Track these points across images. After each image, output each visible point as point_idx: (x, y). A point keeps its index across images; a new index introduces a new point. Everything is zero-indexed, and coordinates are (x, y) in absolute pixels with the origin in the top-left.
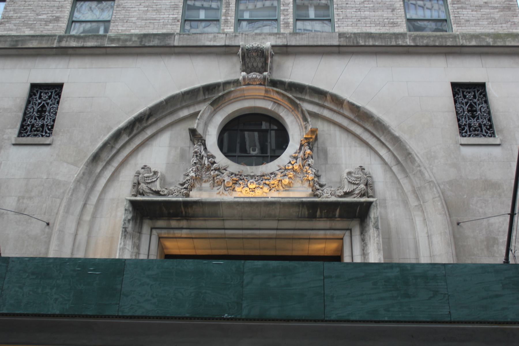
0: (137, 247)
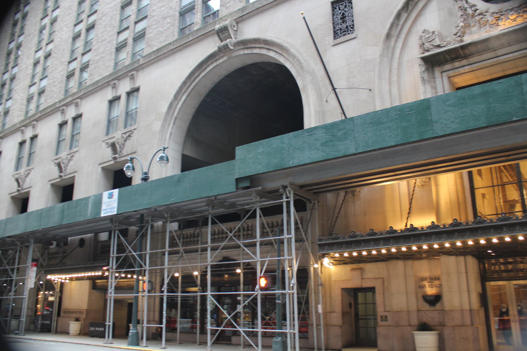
0: (435, 88)
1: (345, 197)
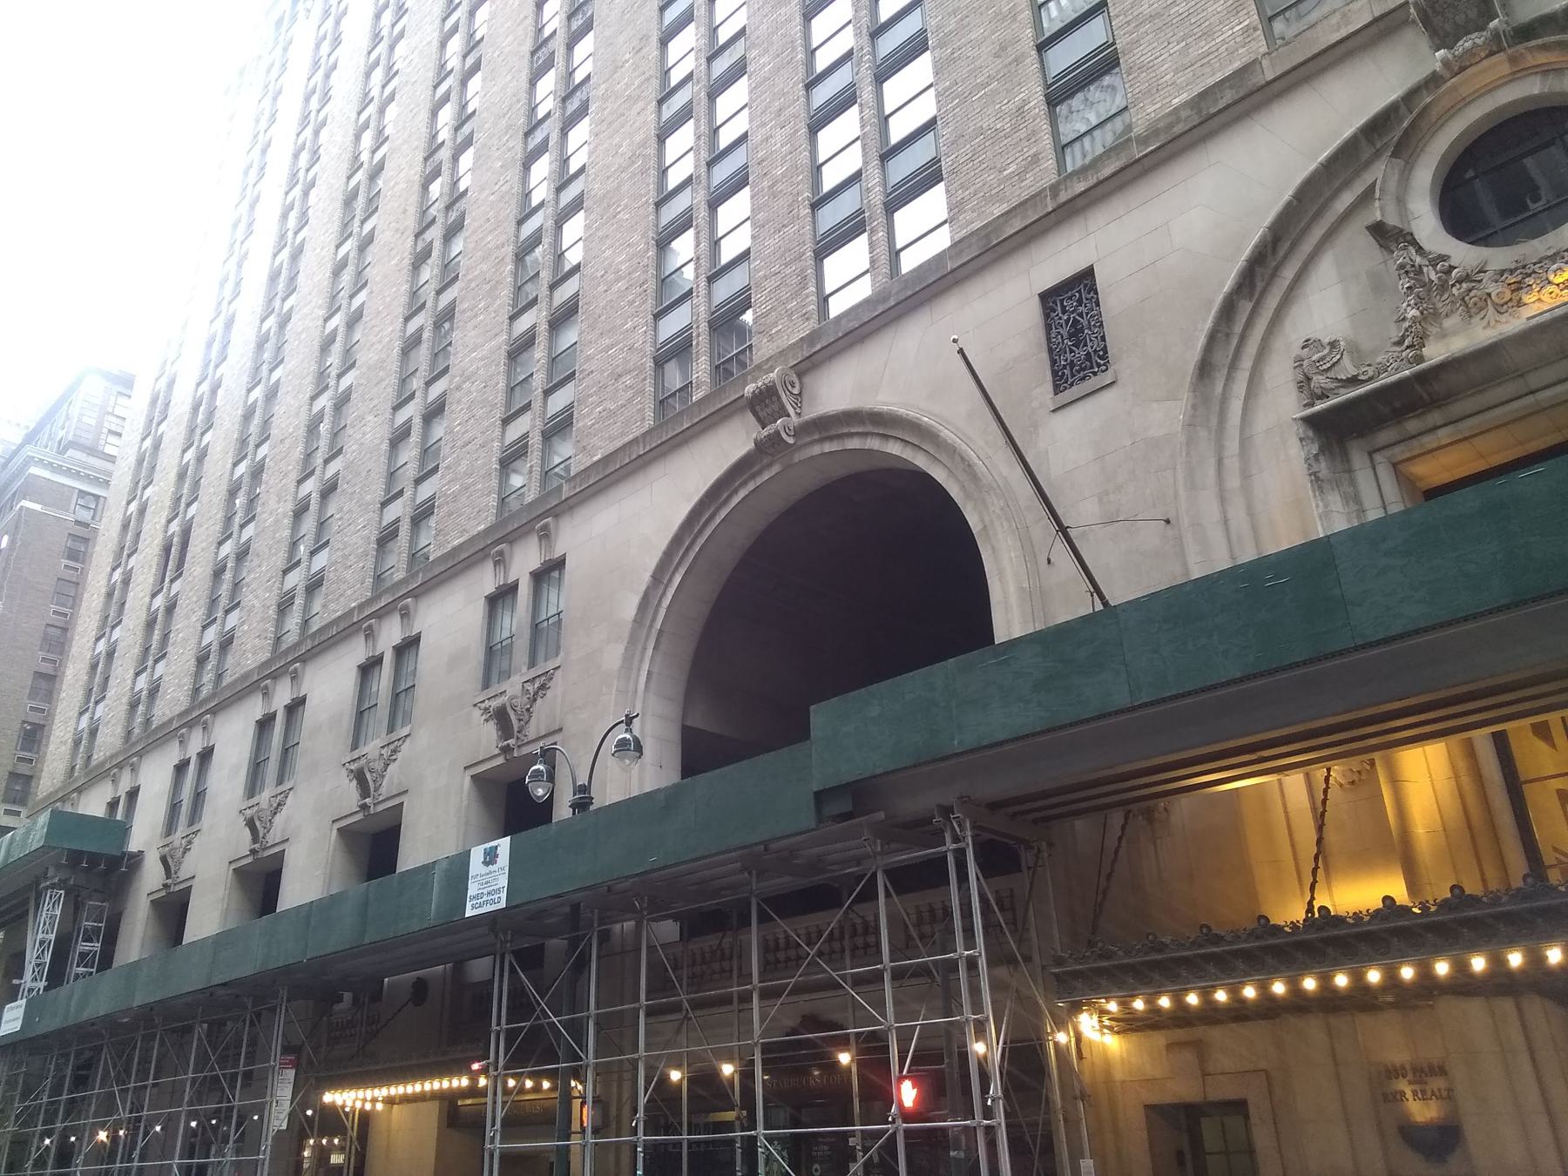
0: (1354, 499)
1: (1123, 828)
